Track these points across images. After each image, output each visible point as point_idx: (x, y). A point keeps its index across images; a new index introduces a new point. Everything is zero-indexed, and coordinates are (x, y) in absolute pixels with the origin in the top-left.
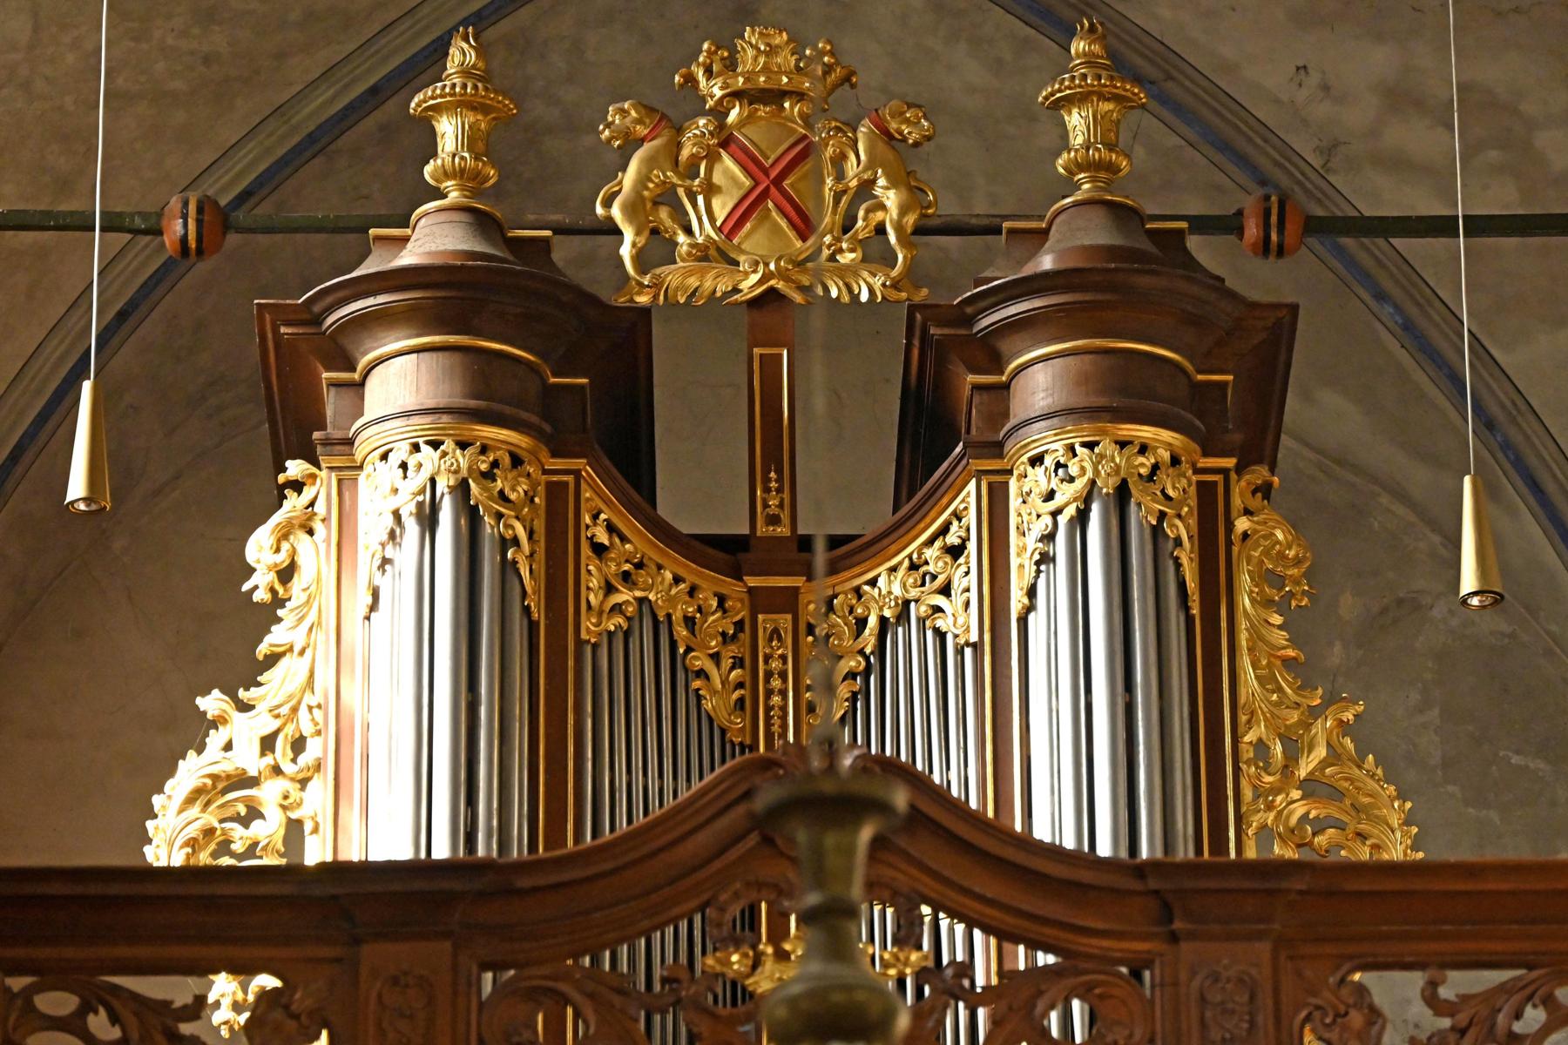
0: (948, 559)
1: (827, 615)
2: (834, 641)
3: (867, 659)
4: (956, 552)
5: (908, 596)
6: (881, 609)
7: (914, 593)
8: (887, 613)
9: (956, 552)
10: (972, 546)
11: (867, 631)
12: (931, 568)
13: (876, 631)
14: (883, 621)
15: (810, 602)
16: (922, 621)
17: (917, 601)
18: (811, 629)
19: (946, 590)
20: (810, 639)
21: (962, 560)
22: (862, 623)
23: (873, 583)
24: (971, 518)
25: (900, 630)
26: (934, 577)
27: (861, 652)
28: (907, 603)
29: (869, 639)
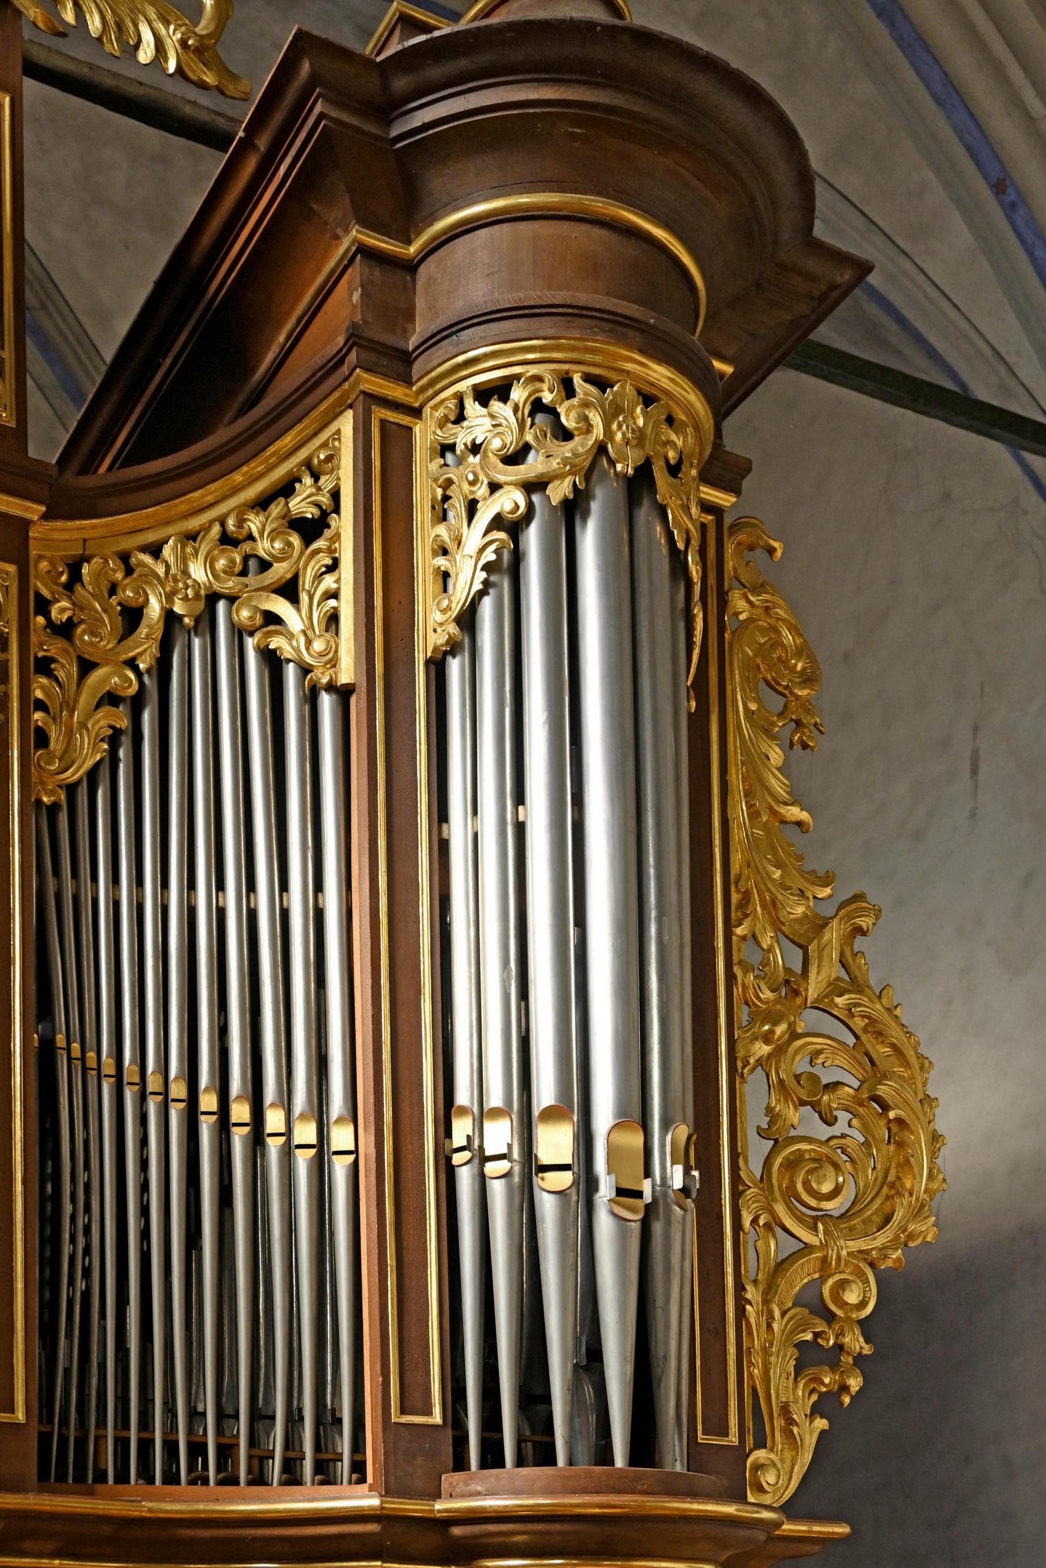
0: (295, 540)
1: (69, 587)
2: (83, 636)
3: (139, 674)
4: (311, 529)
5: (217, 586)
6: (170, 597)
7: (230, 585)
8: (178, 608)
9: (311, 529)
10: (345, 523)
11: (143, 631)
12: (263, 547)
13: (159, 634)
14: (170, 618)
15: (40, 557)
16: (239, 634)
17: (232, 599)
18: (43, 606)
19: (289, 590)
20: (41, 620)
21: (320, 543)
22: (133, 616)
23: (155, 551)
24: (346, 475)
25: (197, 642)
26: (265, 566)
27: (132, 664)
28: (213, 598)
29: (144, 647)
